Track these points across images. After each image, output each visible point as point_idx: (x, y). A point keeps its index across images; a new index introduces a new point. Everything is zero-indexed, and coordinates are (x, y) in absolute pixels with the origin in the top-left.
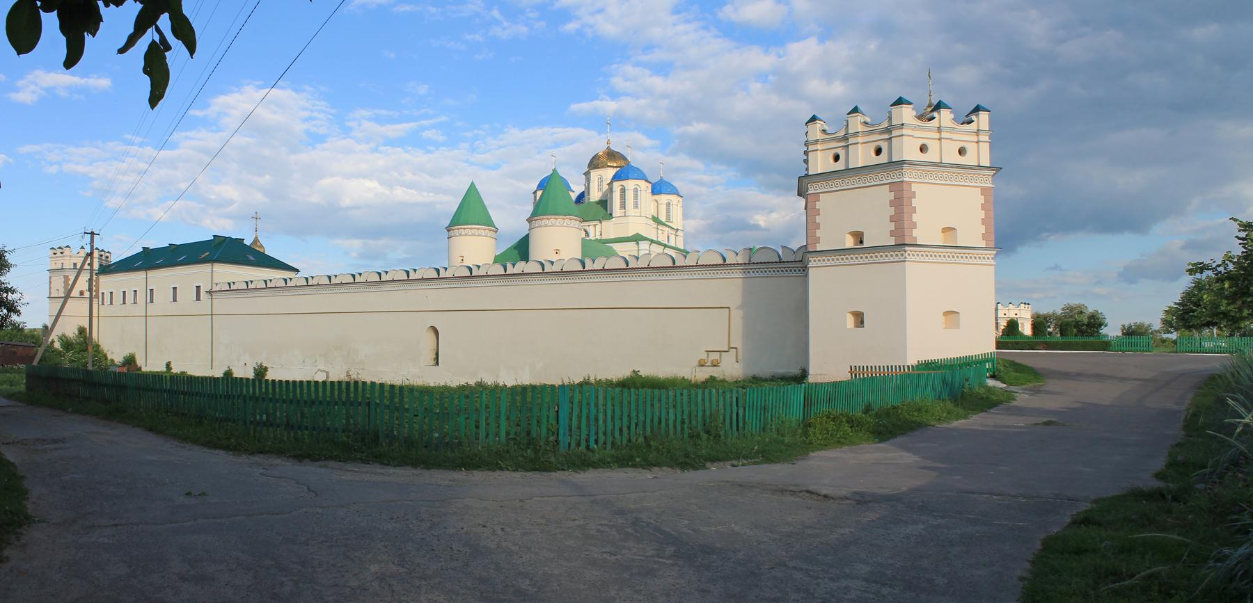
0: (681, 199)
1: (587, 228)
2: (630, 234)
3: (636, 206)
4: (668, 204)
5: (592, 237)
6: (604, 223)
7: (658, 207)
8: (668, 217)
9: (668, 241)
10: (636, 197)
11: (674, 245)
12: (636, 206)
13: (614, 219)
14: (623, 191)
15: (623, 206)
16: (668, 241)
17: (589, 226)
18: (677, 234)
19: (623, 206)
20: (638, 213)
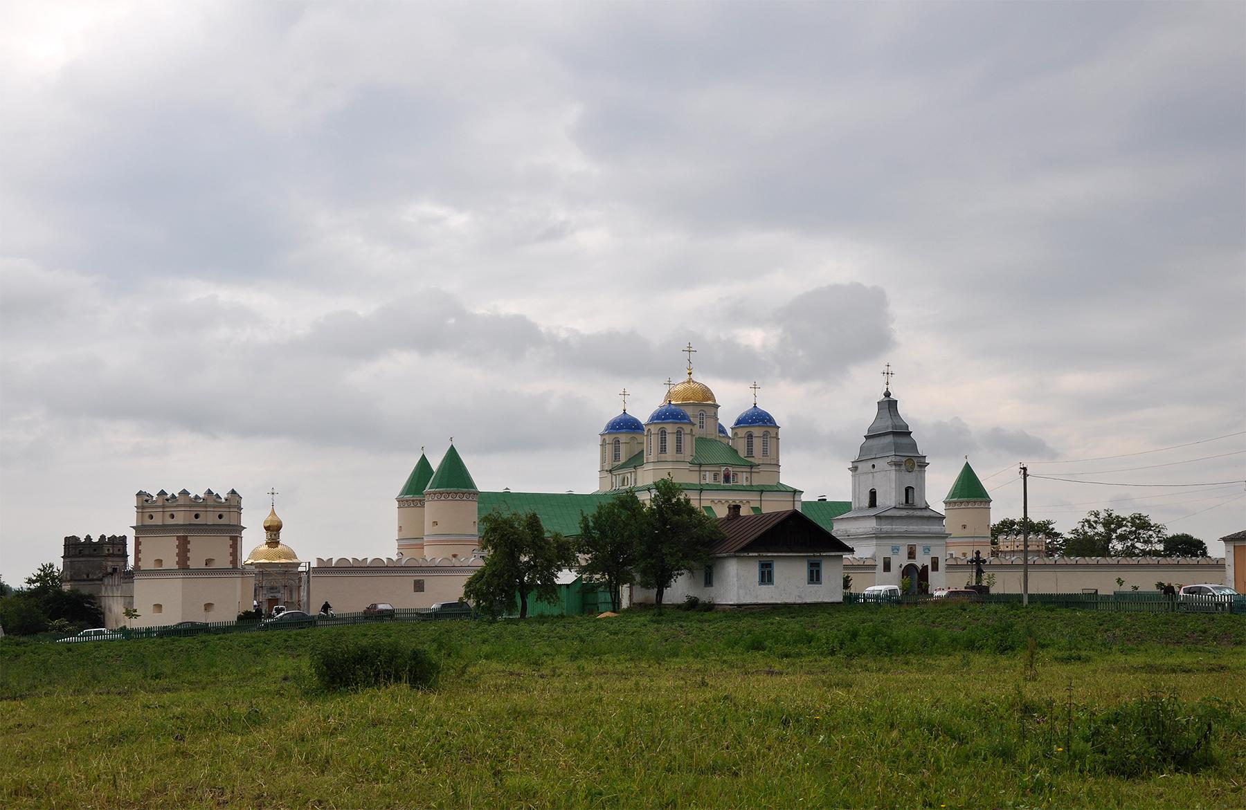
3: (663, 449)
4: (750, 436)
12: (663, 449)
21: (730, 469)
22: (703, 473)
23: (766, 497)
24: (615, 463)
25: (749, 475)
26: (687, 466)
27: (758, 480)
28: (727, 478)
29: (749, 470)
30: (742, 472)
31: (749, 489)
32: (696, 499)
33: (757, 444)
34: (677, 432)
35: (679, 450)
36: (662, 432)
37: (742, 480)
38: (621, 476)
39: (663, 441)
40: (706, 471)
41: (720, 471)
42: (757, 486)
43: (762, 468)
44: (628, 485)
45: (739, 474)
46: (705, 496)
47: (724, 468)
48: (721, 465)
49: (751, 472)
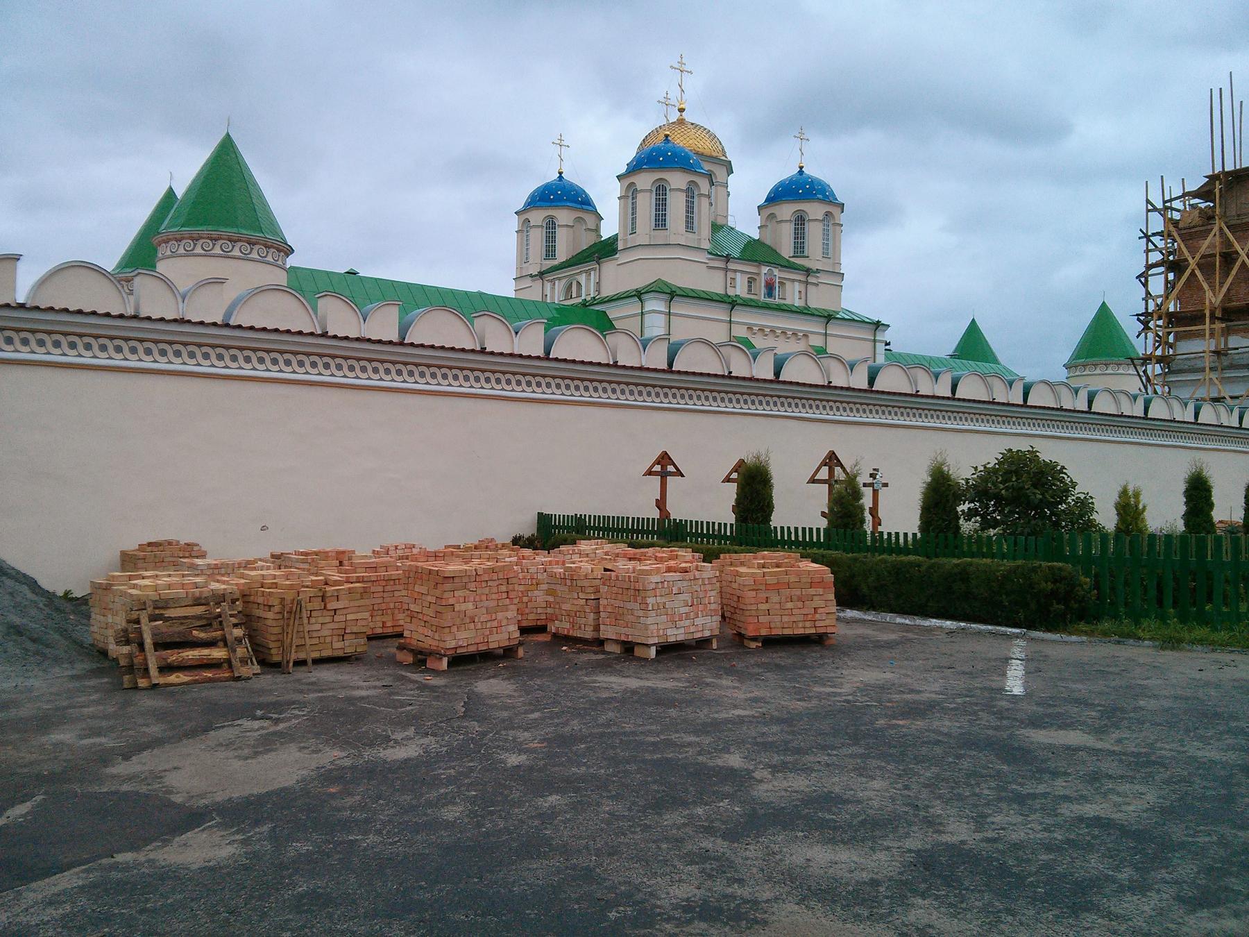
3: (660, 221)
12: (660, 221)
20: (660, 237)
21: (776, 272)
22: (730, 275)
23: (833, 329)
24: (548, 262)
25: (802, 288)
26: (703, 257)
27: (817, 300)
28: (770, 288)
29: (802, 278)
30: (794, 280)
31: (805, 312)
32: (721, 321)
33: (814, 232)
34: (687, 190)
35: (690, 225)
36: (658, 189)
37: (793, 295)
40: (735, 271)
41: (758, 274)
42: (816, 309)
43: (823, 279)
44: (579, 296)
45: (788, 284)
46: (741, 316)
47: (765, 270)
48: (760, 263)
49: (807, 283)
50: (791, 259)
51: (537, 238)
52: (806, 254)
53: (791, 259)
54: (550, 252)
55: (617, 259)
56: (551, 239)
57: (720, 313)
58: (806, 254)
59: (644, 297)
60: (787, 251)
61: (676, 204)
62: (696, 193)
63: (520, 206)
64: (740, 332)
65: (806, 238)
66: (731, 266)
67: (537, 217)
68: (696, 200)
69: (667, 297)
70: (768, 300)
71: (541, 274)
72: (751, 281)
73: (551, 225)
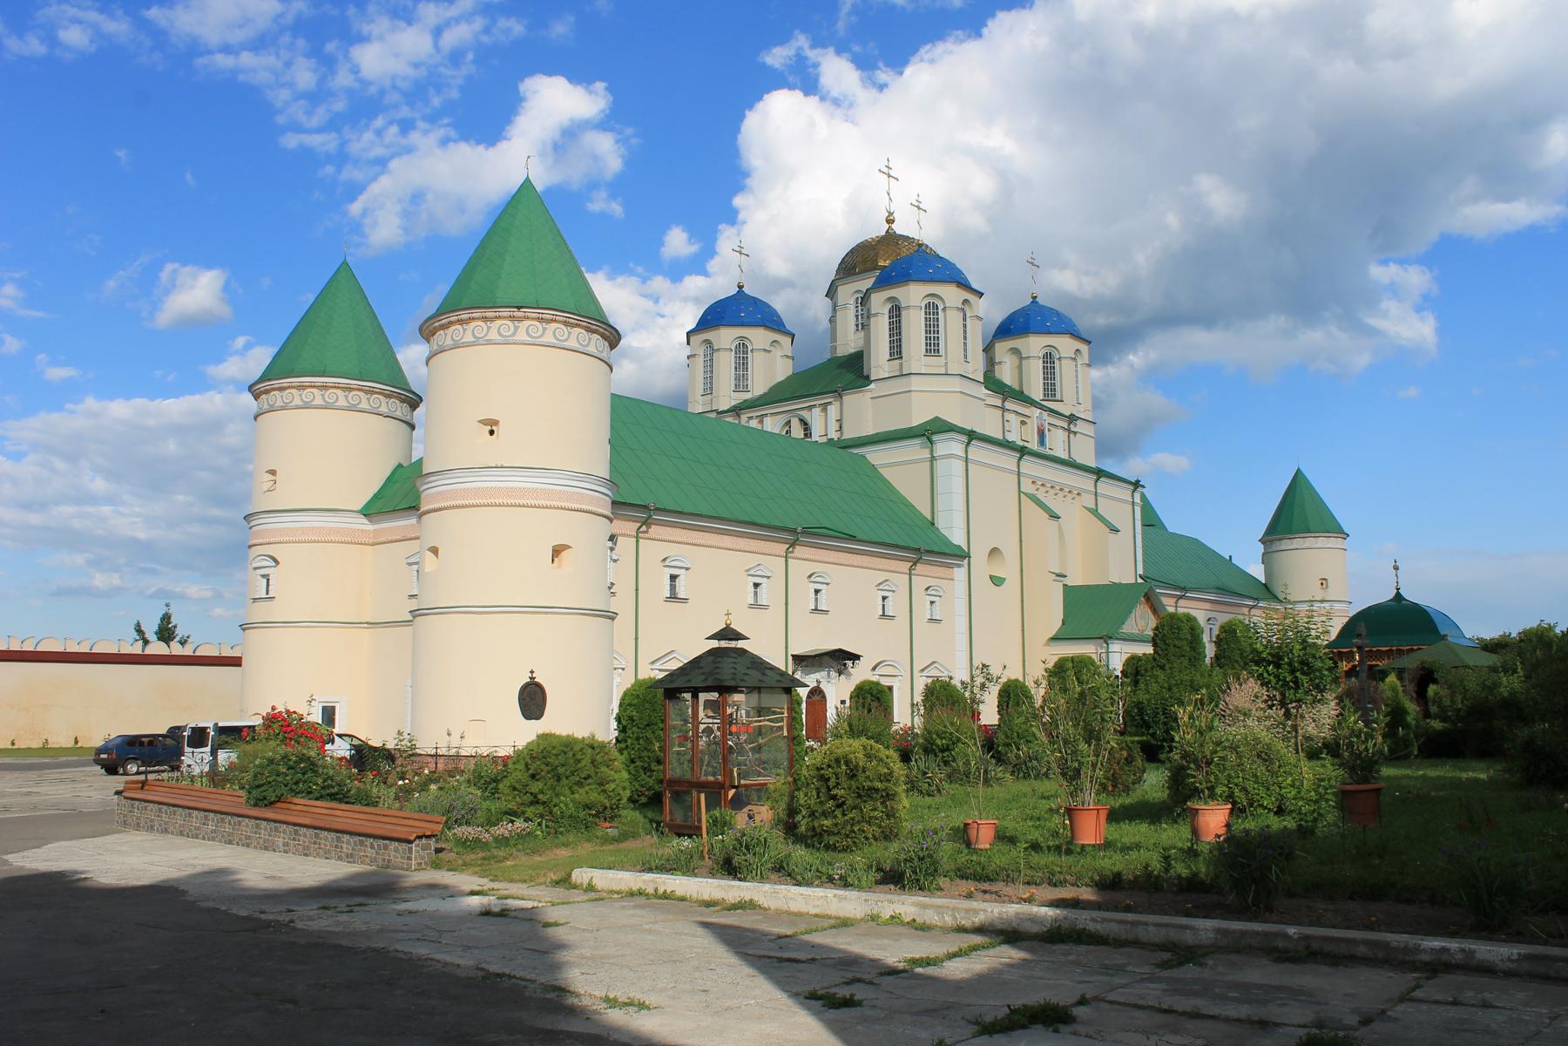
0: (1084, 348)
1: (805, 414)
2: (917, 419)
3: (932, 348)
4: (1049, 359)
5: (816, 436)
6: (850, 399)
7: (1020, 367)
8: (1050, 390)
9: (1042, 441)
10: (932, 327)
11: (1064, 456)
12: (932, 348)
13: (872, 386)
14: (896, 311)
15: (896, 351)
16: (1042, 441)
17: (810, 408)
18: (1073, 428)
19: (896, 351)
20: (935, 364)
28: (1041, 434)
36: (928, 306)
37: (1057, 443)
38: (781, 416)
39: (932, 327)
46: (1030, 467)
50: (1042, 403)
51: (725, 364)
52: (1058, 397)
53: (1043, 403)
54: (741, 383)
55: (871, 391)
56: (742, 364)
57: (1008, 460)
58: (1058, 397)
59: (935, 438)
60: (1037, 393)
61: (950, 325)
62: (968, 315)
63: (692, 325)
64: (1027, 487)
65: (1058, 378)
66: (1008, 405)
67: (726, 337)
68: (968, 319)
69: (965, 439)
70: (1041, 450)
71: (736, 410)
72: (1023, 423)
73: (742, 349)
